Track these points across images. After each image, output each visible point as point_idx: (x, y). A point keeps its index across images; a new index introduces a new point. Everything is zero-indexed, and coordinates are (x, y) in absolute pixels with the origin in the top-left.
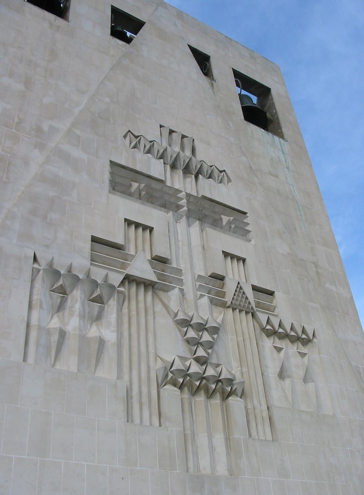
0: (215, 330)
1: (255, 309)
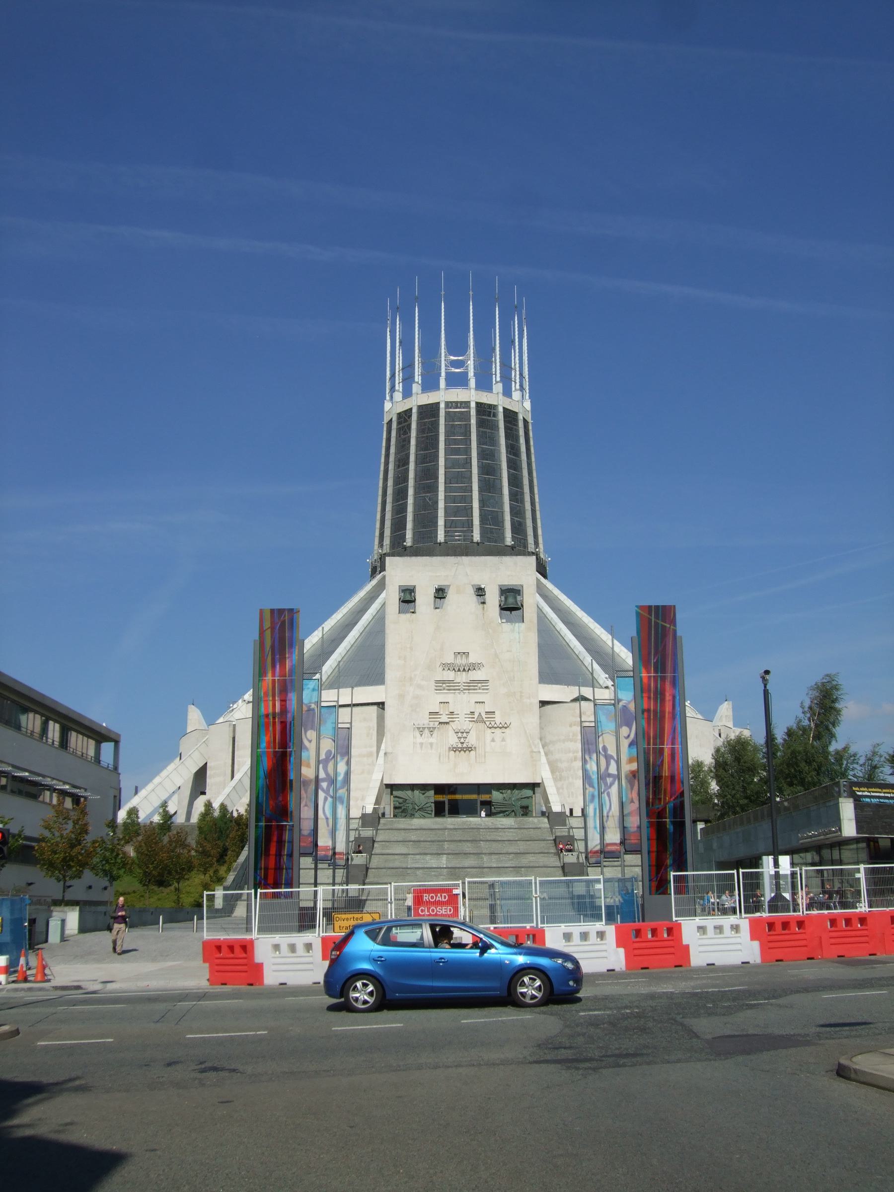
0: (467, 733)
1: (485, 719)
